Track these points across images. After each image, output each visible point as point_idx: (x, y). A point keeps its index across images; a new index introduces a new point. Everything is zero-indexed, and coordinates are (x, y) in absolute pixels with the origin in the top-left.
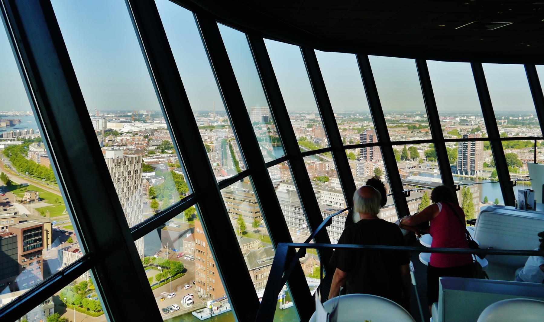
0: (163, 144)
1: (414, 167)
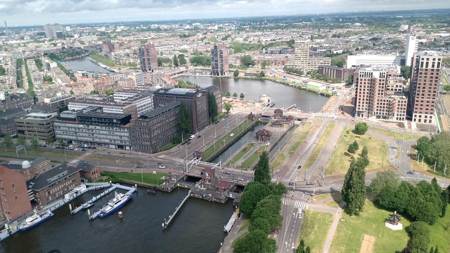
1: (183, 72)
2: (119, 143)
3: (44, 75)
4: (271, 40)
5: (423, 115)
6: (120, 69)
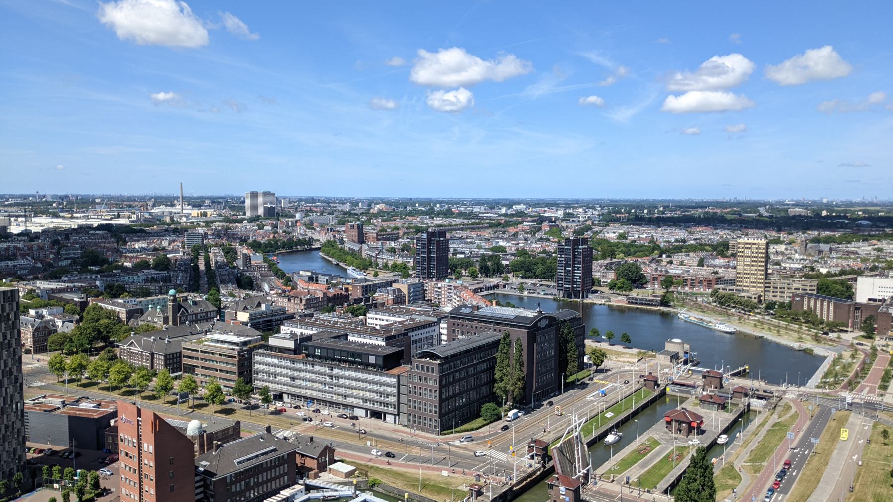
0: (82, 257)
2: (376, 407)
3: (239, 275)
4: (677, 241)
6: (376, 275)
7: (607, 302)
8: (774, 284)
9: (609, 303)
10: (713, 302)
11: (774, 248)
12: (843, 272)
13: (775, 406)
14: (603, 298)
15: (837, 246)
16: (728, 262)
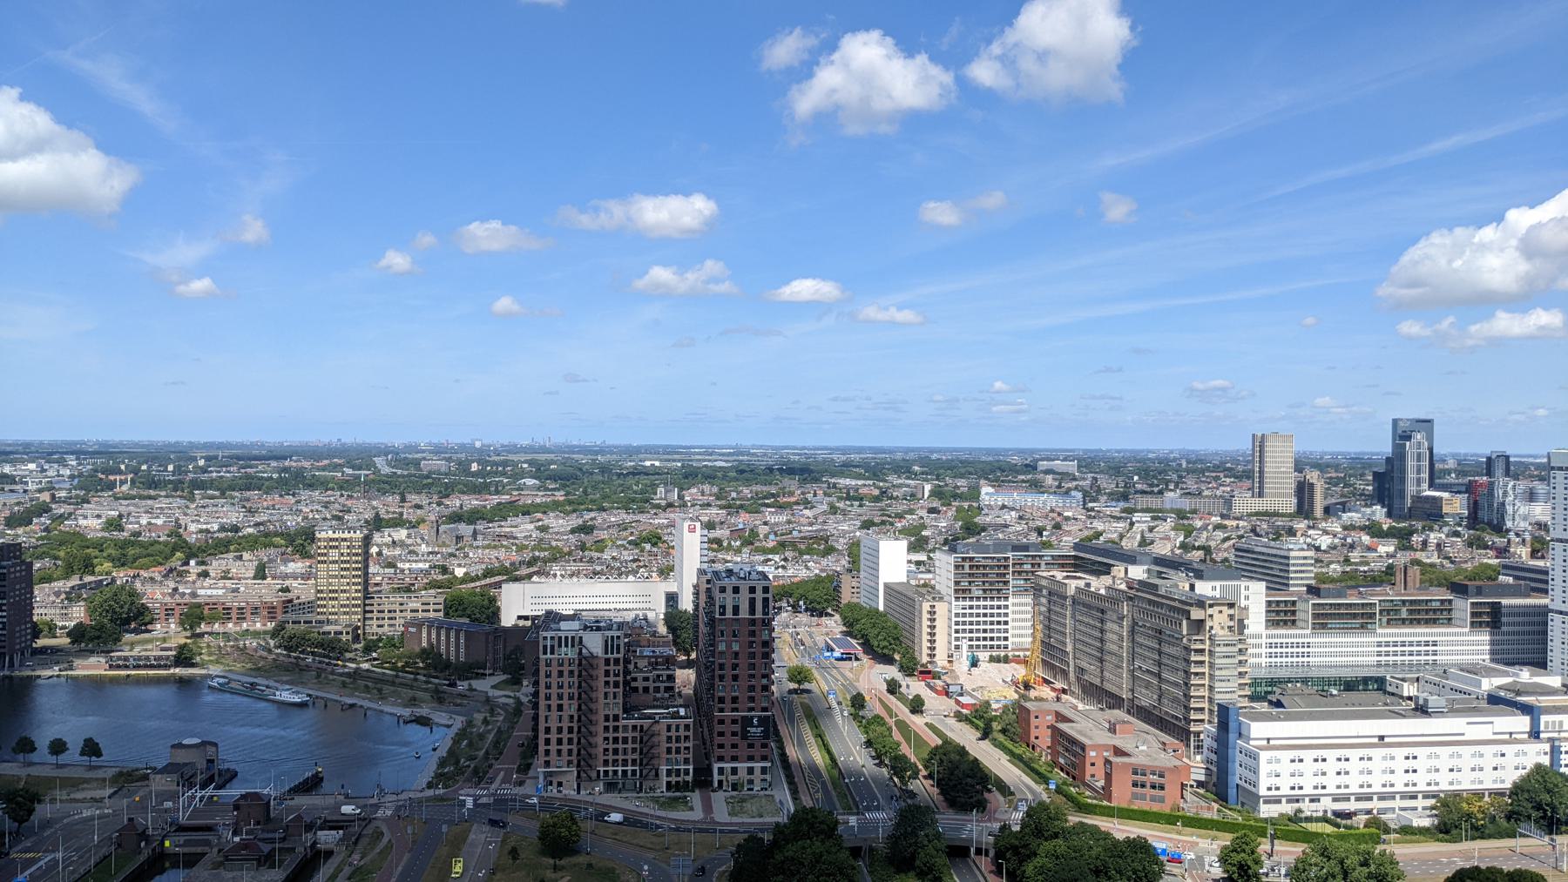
4: (222, 529)
5: (742, 766)
7: (66, 670)
8: (379, 605)
9: (70, 673)
10: (276, 647)
11: (389, 536)
12: (488, 573)
13: (357, 840)
14: (57, 663)
15: (487, 525)
16: (310, 567)
